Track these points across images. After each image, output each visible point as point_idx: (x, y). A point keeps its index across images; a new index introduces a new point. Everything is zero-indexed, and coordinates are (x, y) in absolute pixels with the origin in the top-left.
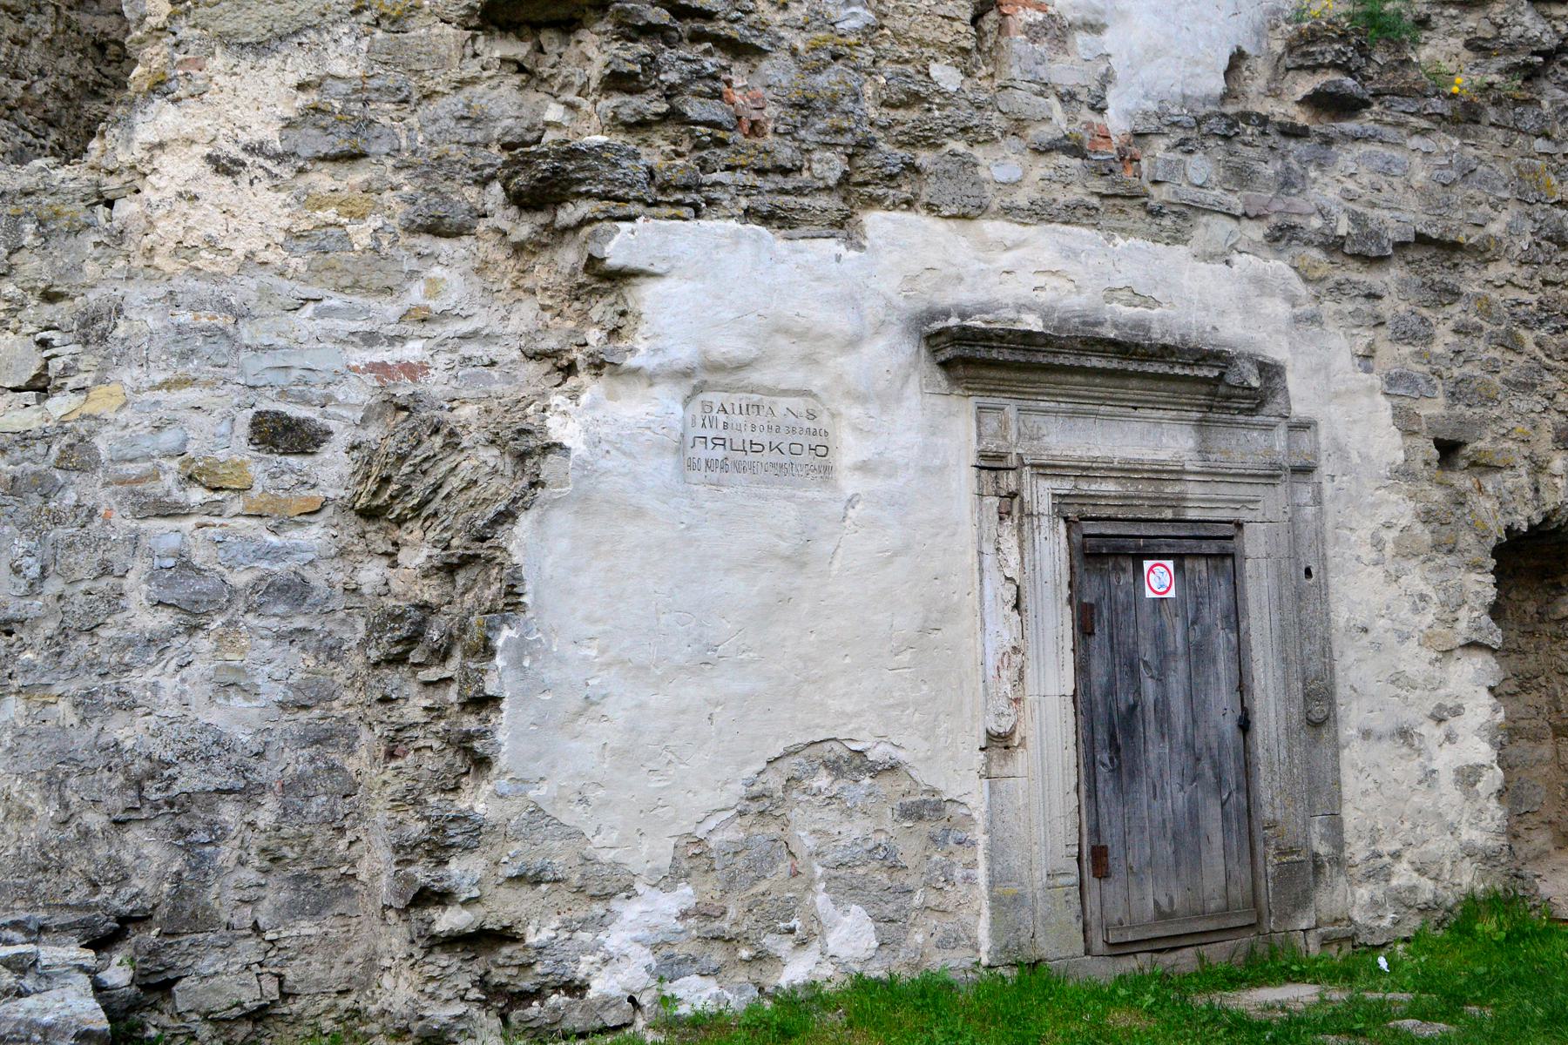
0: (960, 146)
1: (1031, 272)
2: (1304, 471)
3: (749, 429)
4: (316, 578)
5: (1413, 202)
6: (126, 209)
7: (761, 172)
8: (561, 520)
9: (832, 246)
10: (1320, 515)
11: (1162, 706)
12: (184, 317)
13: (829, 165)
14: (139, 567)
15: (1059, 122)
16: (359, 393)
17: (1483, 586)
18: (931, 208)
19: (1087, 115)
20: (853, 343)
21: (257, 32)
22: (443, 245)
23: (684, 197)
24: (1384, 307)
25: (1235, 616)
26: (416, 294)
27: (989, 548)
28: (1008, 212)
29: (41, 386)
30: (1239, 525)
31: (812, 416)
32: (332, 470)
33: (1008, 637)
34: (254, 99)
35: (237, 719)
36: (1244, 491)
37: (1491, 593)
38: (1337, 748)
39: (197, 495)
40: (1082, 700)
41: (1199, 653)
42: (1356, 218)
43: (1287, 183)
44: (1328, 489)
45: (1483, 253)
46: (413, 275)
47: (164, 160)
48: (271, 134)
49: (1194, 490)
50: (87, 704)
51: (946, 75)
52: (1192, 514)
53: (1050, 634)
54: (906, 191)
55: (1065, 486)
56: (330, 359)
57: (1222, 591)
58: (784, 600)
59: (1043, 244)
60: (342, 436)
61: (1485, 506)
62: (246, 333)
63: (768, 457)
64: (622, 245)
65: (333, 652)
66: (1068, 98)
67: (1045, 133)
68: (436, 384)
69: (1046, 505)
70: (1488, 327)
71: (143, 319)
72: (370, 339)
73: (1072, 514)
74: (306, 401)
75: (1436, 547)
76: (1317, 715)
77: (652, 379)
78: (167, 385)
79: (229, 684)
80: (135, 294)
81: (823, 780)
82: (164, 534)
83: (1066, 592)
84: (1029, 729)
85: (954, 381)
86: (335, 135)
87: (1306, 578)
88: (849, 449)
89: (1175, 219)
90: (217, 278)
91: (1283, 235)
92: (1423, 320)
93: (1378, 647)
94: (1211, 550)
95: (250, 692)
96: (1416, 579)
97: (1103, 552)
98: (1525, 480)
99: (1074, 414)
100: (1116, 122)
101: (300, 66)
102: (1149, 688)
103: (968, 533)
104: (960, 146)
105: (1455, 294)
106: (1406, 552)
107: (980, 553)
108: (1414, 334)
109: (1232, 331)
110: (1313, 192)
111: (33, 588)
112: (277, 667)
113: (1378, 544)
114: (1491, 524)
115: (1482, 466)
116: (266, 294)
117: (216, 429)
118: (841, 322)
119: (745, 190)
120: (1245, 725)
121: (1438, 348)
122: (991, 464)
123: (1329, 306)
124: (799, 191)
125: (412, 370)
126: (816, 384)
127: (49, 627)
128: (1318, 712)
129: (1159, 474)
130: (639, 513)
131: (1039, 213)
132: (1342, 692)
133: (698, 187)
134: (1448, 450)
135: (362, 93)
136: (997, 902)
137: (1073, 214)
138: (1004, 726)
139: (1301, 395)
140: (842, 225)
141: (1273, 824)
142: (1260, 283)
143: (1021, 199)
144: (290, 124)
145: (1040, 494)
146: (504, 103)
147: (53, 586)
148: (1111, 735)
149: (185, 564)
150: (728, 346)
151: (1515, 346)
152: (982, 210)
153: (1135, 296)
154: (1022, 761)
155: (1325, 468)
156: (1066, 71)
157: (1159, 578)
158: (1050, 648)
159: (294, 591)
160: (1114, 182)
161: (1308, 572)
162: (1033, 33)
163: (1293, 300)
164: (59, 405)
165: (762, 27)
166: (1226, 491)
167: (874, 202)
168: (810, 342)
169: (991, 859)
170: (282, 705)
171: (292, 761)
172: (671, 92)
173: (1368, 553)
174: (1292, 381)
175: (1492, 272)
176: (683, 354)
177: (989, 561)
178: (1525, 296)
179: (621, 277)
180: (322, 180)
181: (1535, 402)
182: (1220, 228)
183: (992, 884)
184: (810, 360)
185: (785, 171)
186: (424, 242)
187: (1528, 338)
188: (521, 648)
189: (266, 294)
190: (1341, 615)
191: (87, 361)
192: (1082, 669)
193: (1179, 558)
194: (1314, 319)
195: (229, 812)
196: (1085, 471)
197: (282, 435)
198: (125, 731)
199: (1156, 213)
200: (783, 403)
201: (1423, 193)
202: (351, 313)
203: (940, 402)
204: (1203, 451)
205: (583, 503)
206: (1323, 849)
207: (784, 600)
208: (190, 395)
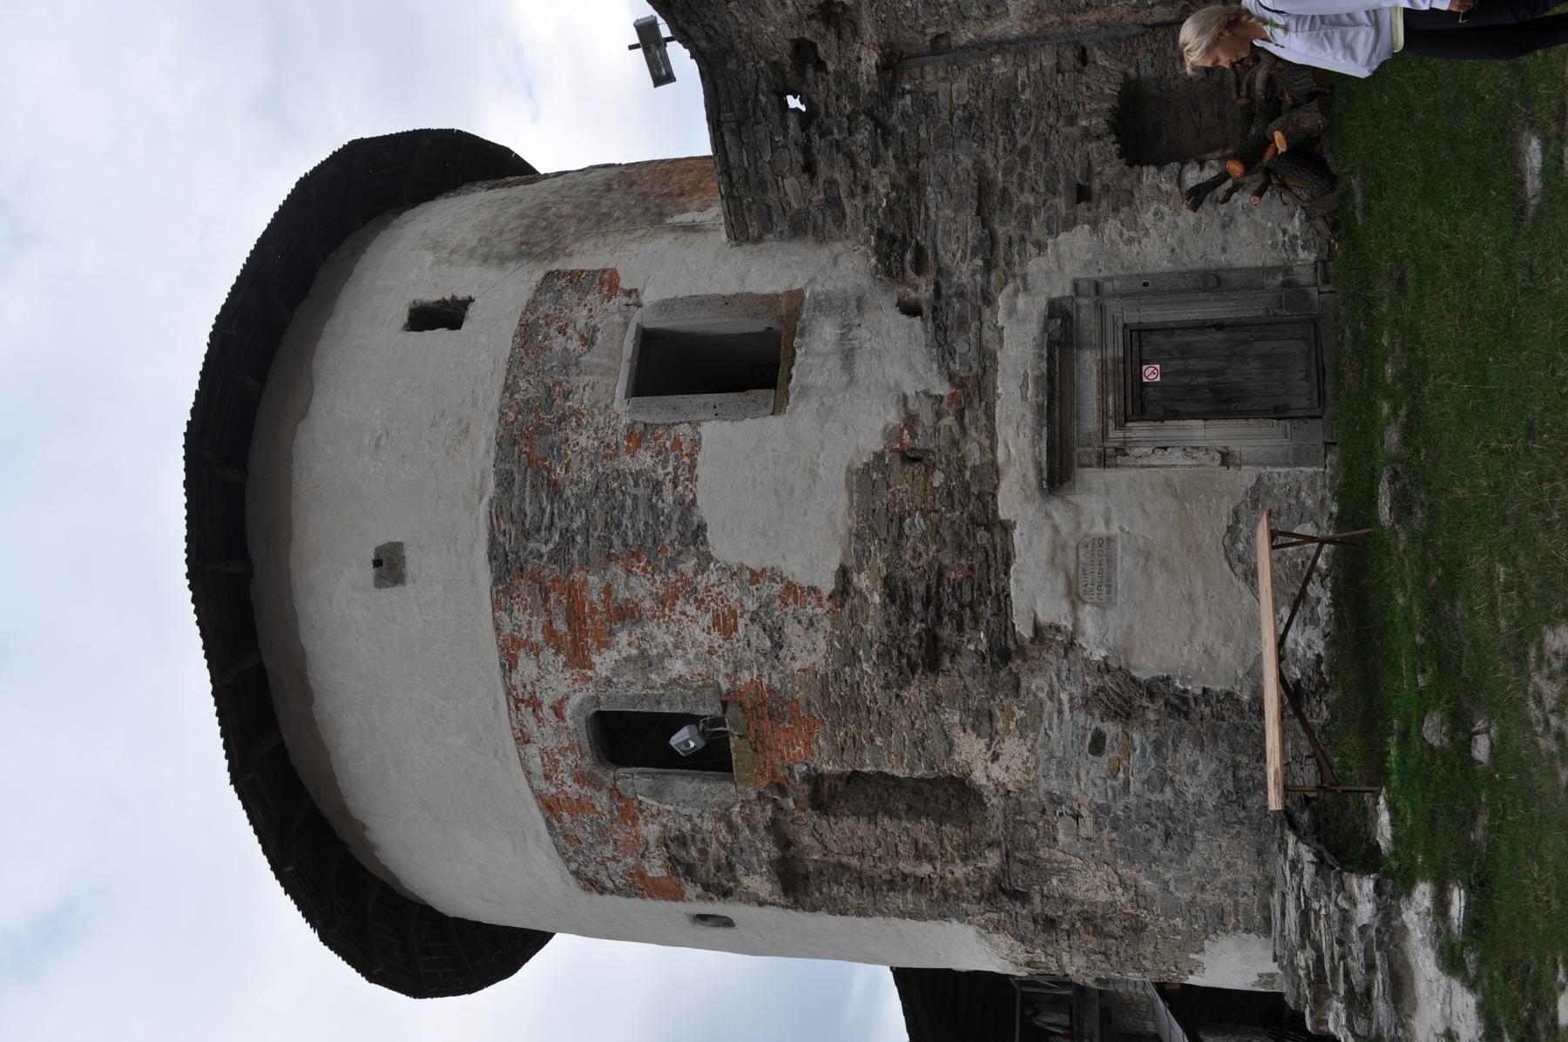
0: (968, 474)
1: (1016, 442)
2: (1097, 286)
3: (1090, 573)
4: (1153, 737)
5: (961, 218)
6: (1010, 787)
7: (989, 567)
8: (1133, 661)
9: (1016, 533)
10: (1117, 277)
11: (1210, 372)
12: (1053, 773)
13: (982, 536)
14: (1149, 795)
15: (948, 420)
16: (1081, 718)
17: (1149, 172)
18: (996, 487)
19: (944, 405)
20: (1056, 529)
21: (944, 744)
22: (1023, 684)
24: (1015, 235)
25: (1166, 329)
26: (1043, 695)
27: (1139, 462)
28: (993, 449)
29: (1077, 817)
30: (1125, 326)
31: (1086, 546)
32: (1111, 729)
33: (1179, 453)
35: (1206, 768)
36: (1109, 326)
37: (1153, 169)
38: (1231, 269)
39: (1121, 775)
40: (1206, 416)
41: (1186, 352)
42: (974, 254)
43: (961, 295)
44: (1105, 273)
45: (981, 170)
46: (1035, 696)
47: (994, 775)
48: (983, 742)
49: (1110, 354)
50: (1198, 814)
51: (938, 479)
52: (1121, 354)
53: (1177, 433)
54: (989, 499)
55: (1111, 423)
56: (1066, 727)
57: (1157, 338)
58: (1164, 561)
59: (1005, 432)
60: (1098, 723)
61: (1109, 171)
62: (1059, 754)
63: (1105, 566)
64: (1024, 630)
65: (1181, 731)
66: (939, 415)
67: (956, 429)
68: (1077, 690)
69: (1119, 434)
70: (1019, 170)
71: (1055, 785)
72: (1060, 712)
73: (1123, 420)
74: (1084, 736)
75: (1130, 204)
76: (1213, 282)
77: (1076, 620)
78: (1079, 780)
79: (1193, 769)
80: (1043, 786)
81: (1240, 546)
82: (1135, 786)
83: (1158, 423)
84: (1220, 444)
85: (1068, 479)
86: (982, 721)
87: (1148, 287)
88: (1100, 529)
89: (987, 359)
90: (1038, 761)
91: (988, 300)
92: (1019, 211)
93: (1181, 242)
94: (1140, 341)
95: (1196, 763)
96: (1147, 218)
97: (1139, 404)
98: (1093, 145)
99: (1078, 416)
100: (944, 389)
101: (957, 732)
102: (1201, 380)
103: (1134, 472)
104: (968, 474)
105: (1005, 190)
106: (1134, 225)
107: (1142, 467)
108: (1026, 214)
109: (1034, 328)
110: (964, 279)
111: (1154, 826)
112: (1187, 753)
113: (1130, 241)
114: (1118, 168)
115: (1089, 172)
116: (1044, 746)
118: (1047, 533)
119: (997, 575)
120: (1219, 326)
121: (1032, 201)
122: (1103, 461)
123: (1017, 269)
124: (995, 551)
125: (1071, 699)
126: (1073, 543)
127: (1169, 823)
128: (1213, 282)
129: (1103, 373)
130: (1130, 627)
131: (992, 434)
132: (1201, 265)
133: (998, 595)
134: (1083, 194)
135: (966, 710)
136: (1296, 464)
137: (991, 417)
138: (1218, 456)
139: (1062, 289)
140: (1007, 527)
141: (1267, 310)
142: (1012, 311)
143: (986, 443)
144: (979, 736)
145: (1115, 434)
146: (966, 663)
147: (1153, 820)
148: (1223, 403)
149: (1147, 781)
150: (1061, 585)
151: (1025, 151)
152: (994, 463)
153: (1024, 386)
154: (1234, 447)
155: (1095, 275)
156: (926, 417)
157: (1151, 373)
158: (1183, 433)
159: (1158, 746)
160: (972, 392)
161: (1145, 284)
162: (914, 435)
163: (1017, 291)
164: (1084, 812)
165: (930, 565)
166: (1109, 336)
167: (995, 513)
168: (1057, 547)
169: (1276, 465)
170: (1202, 751)
171: (1223, 747)
172: (962, 606)
173: (1135, 248)
174: (1056, 294)
175: (991, 165)
176: (1065, 606)
177: (1145, 462)
178: (1001, 143)
179: (1038, 629)
180: (1000, 725)
181: (1053, 137)
182: (988, 335)
183: (1289, 465)
184: (1064, 548)
185: (987, 555)
186: (1023, 692)
187: (1022, 142)
188: (1183, 680)
189: (1044, 746)
190: (1166, 266)
191: (1068, 803)
192: (1193, 417)
193: (1142, 362)
194: (1024, 278)
195: (1242, 774)
196: (1104, 412)
198: (1210, 803)
199: (984, 369)
200: (1082, 559)
201: (956, 211)
202: (1050, 719)
203: (1078, 485)
204: (1091, 346)
205: (1127, 651)
206: (1280, 278)
207: (1164, 561)
208: (1083, 774)
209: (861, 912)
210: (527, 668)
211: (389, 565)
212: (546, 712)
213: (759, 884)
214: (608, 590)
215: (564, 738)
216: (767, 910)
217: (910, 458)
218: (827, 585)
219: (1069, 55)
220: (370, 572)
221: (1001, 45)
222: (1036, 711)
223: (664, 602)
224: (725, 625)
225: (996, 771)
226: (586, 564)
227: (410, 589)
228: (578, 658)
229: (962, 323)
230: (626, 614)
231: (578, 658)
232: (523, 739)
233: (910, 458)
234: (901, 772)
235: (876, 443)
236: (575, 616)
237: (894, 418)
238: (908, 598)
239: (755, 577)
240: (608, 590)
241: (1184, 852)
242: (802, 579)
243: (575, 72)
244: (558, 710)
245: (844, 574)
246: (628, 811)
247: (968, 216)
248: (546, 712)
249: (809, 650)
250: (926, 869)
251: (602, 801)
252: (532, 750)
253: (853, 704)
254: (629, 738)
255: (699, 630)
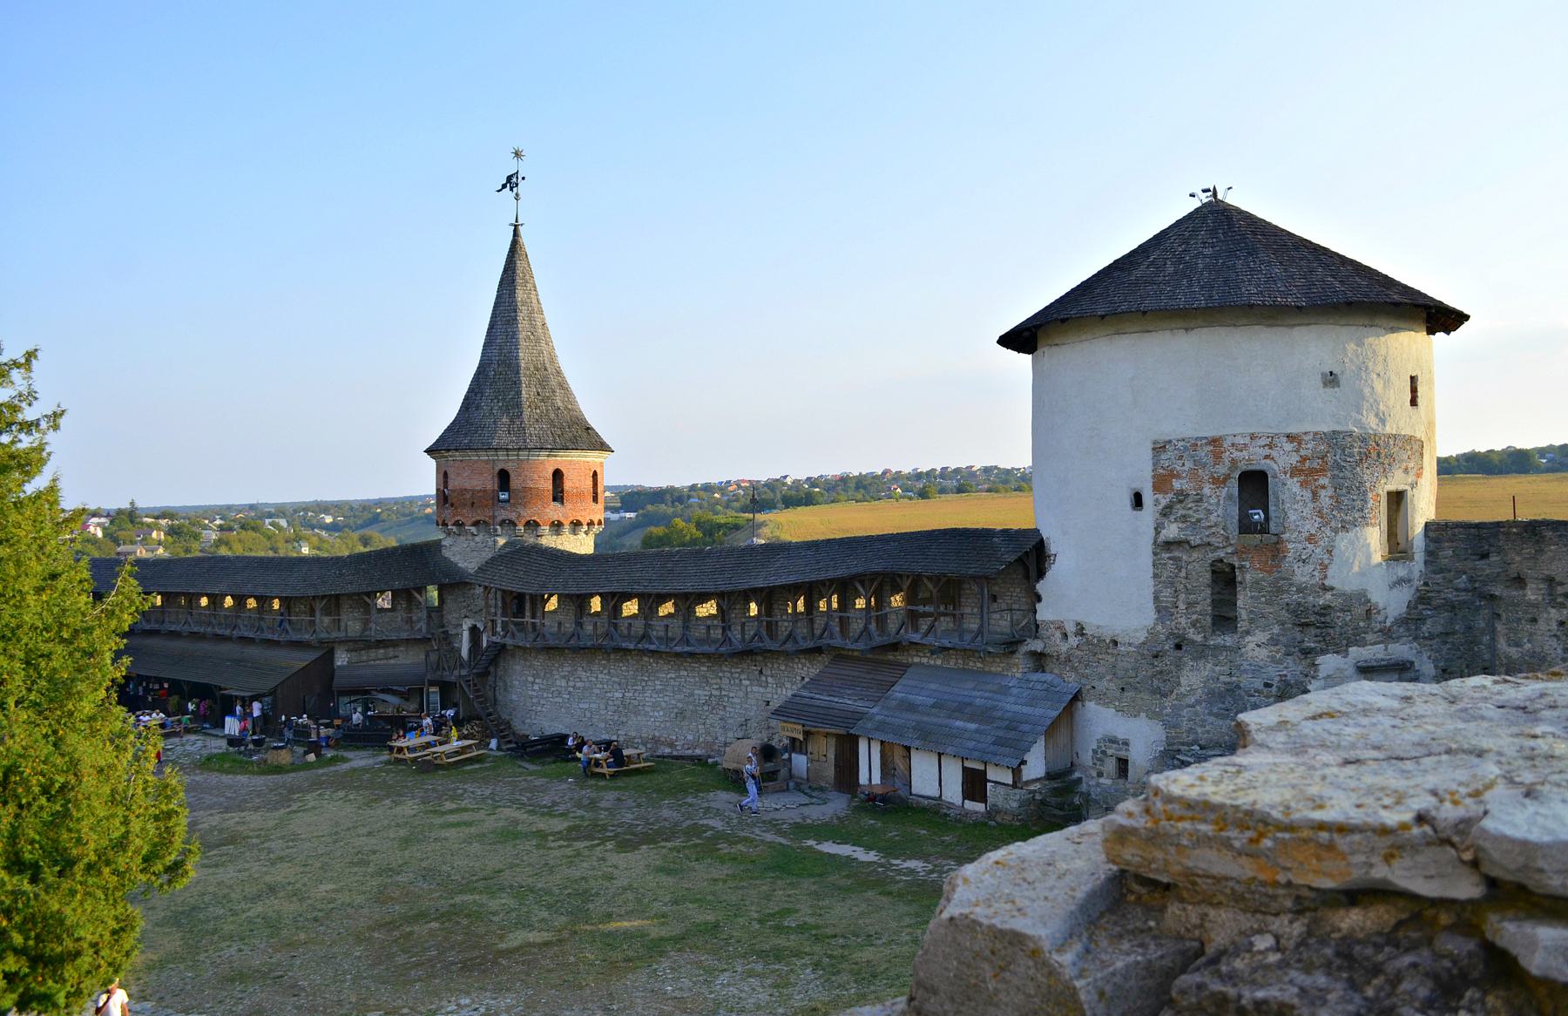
23: (1323, 652)
32: (1274, 689)
34: (1261, 637)
45: (1454, 633)
56: (1273, 673)
86: (1274, 641)
91: (1416, 638)
117: (1259, 684)
146: (1299, 636)
156: (1380, 618)
160: (1387, 635)
197: (1267, 685)
209: (1155, 576)
210: (1288, 447)
211: (1331, 380)
212: (1267, 451)
213: (1172, 531)
214: (1323, 487)
215: (1254, 457)
216: (1153, 532)
217: (1368, 612)
218: (1327, 583)
219: (1487, 664)
220: (1327, 371)
221: (1493, 639)
222: (1280, 662)
223: (1320, 513)
224: (1311, 539)
225: (1252, 645)
226: (1334, 477)
227: (1321, 390)
228: (1295, 472)
229: (1408, 630)
230: (1315, 495)
231: (1295, 472)
232: (1253, 437)
233: (1368, 612)
234: (1239, 603)
235: (1373, 600)
236: (1312, 471)
237: (1381, 606)
238: (1324, 615)
239: (1330, 552)
240: (1323, 487)
241: (1217, 715)
242: (1330, 573)
243: (1467, 403)
244: (1267, 457)
245: (1332, 589)
246: (1219, 482)
247: (1440, 629)
248: (1267, 451)
249: (1302, 574)
250: (1182, 606)
251: (1222, 470)
252: (1247, 440)
253: (1280, 591)
254: (1254, 484)
255: (1310, 527)
